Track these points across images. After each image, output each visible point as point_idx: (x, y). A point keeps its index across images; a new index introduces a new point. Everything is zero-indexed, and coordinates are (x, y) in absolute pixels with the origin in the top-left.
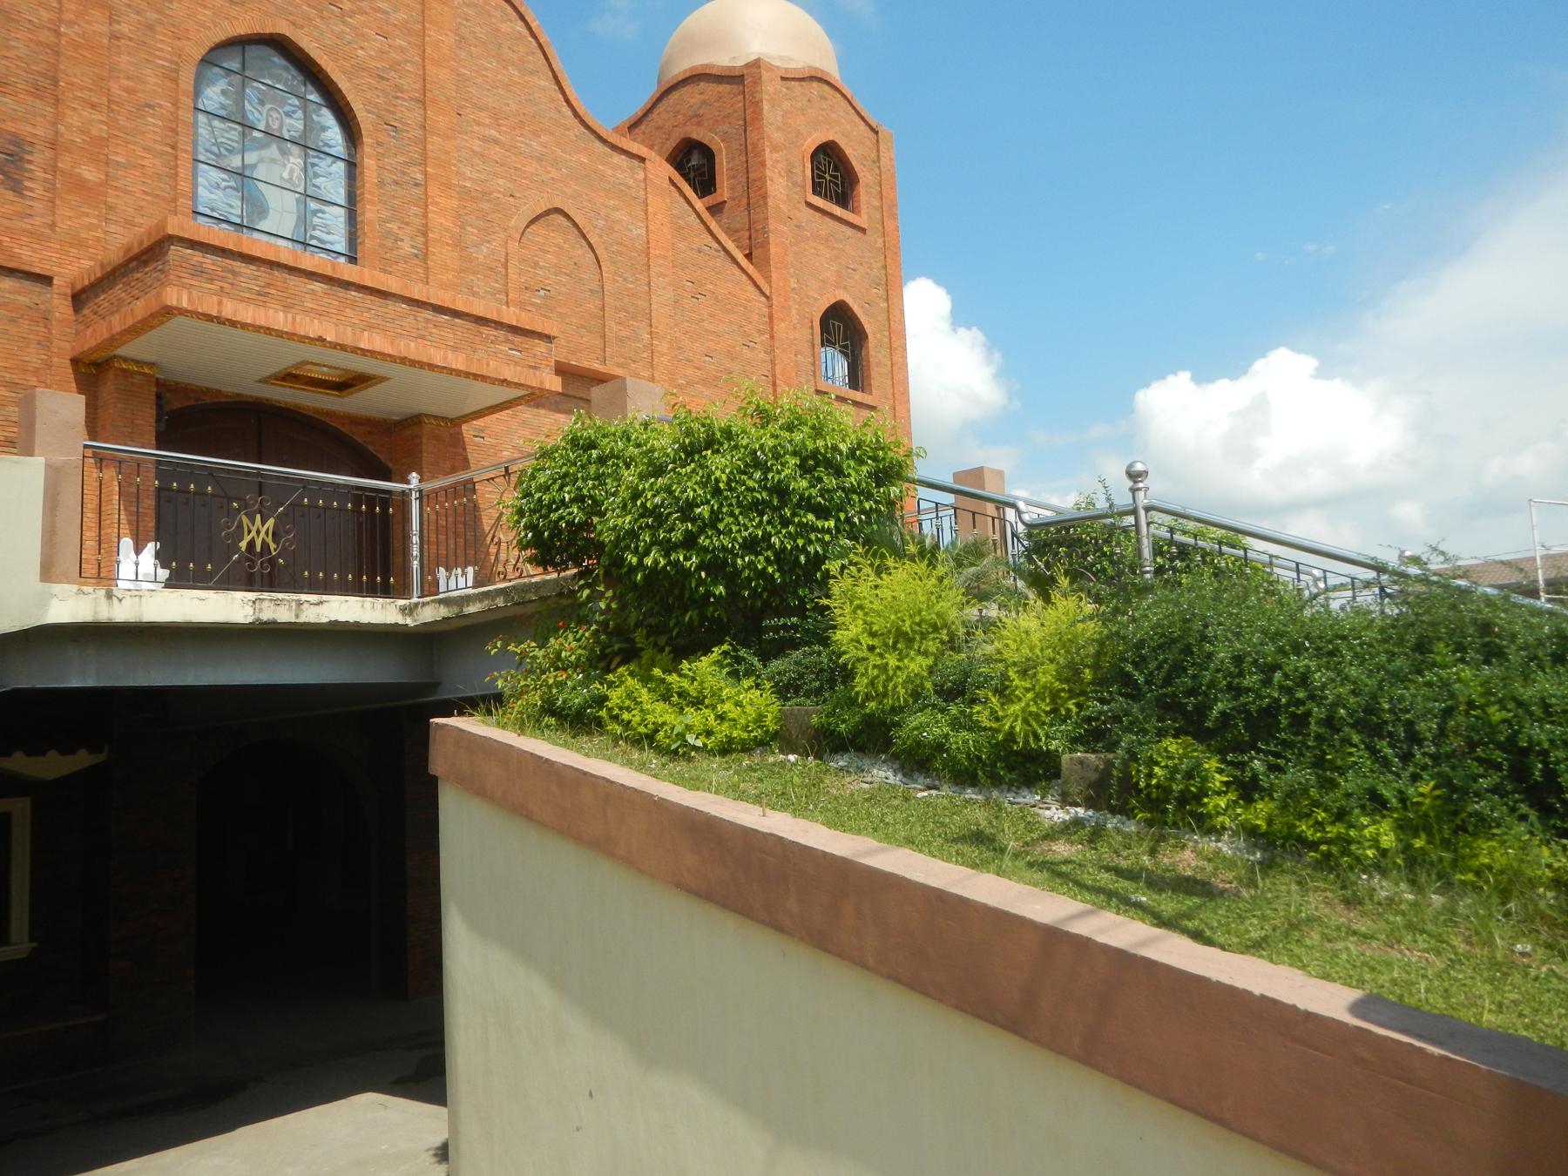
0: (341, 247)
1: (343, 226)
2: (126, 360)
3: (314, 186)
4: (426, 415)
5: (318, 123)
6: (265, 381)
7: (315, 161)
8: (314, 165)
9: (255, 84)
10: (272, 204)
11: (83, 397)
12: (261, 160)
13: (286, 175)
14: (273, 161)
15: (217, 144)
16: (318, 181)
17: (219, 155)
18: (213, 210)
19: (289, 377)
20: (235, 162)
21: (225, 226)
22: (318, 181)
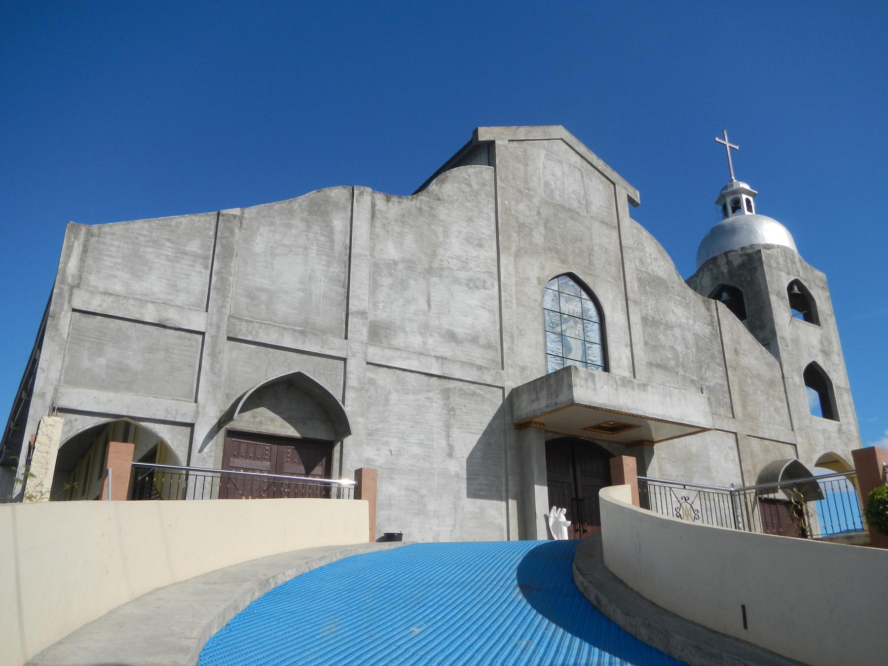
0: (599, 363)
1: (599, 353)
2: (535, 423)
3: (587, 336)
4: (646, 441)
5: (586, 308)
6: (585, 429)
7: (587, 325)
8: (587, 327)
9: (564, 295)
10: (572, 347)
11: (634, 458)
12: (567, 328)
13: (577, 333)
14: (572, 327)
15: (552, 323)
16: (588, 334)
17: (552, 328)
18: (553, 352)
19: (599, 428)
20: (559, 329)
21: (557, 358)
22: (589, 334)
